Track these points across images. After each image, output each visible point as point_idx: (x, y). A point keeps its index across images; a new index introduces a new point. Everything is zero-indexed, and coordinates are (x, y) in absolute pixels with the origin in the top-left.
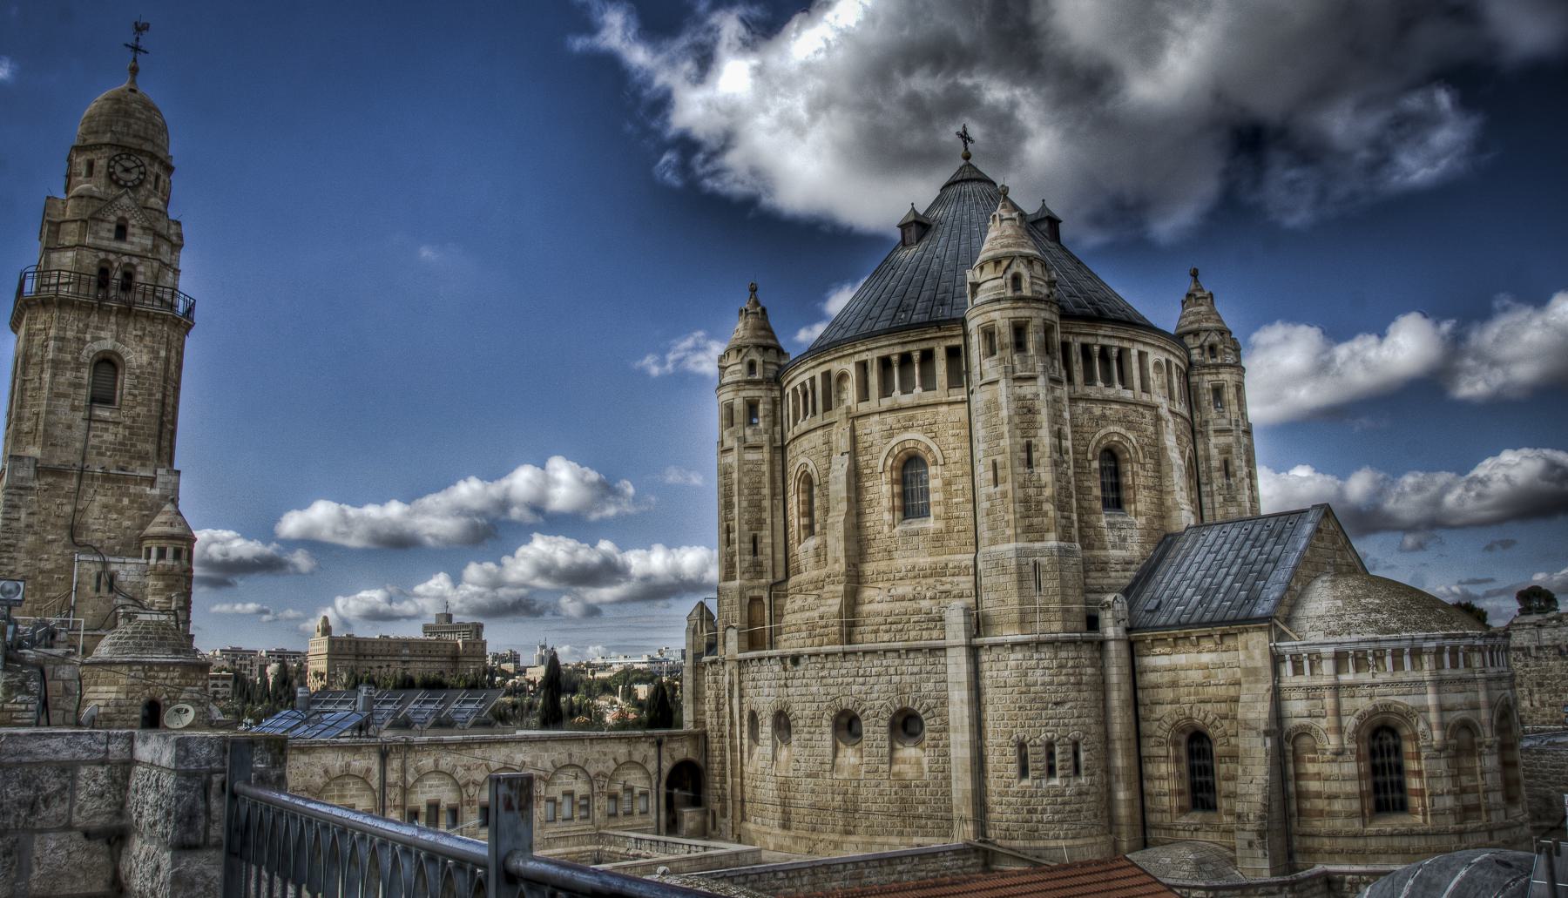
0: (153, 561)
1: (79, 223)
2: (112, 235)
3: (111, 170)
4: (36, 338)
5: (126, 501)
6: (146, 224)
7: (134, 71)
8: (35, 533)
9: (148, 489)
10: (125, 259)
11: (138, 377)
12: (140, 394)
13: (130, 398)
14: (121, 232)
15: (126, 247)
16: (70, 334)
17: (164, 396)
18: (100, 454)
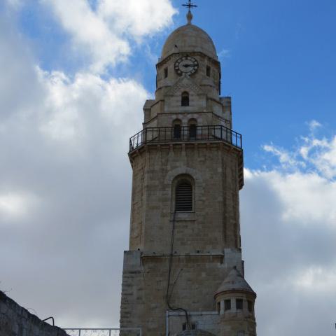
0: (222, 312)
1: (160, 103)
2: (180, 104)
3: (177, 68)
4: (138, 176)
5: (204, 275)
6: (200, 92)
7: (190, 17)
8: (144, 303)
9: (219, 264)
10: (190, 116)
11: (204, 188)
12: (207, 199)
13: (200, 202)
14: (185, 101)
15: (187, 108)
16: (157, 168)
17: (225, 199)
18: (183, 244)
